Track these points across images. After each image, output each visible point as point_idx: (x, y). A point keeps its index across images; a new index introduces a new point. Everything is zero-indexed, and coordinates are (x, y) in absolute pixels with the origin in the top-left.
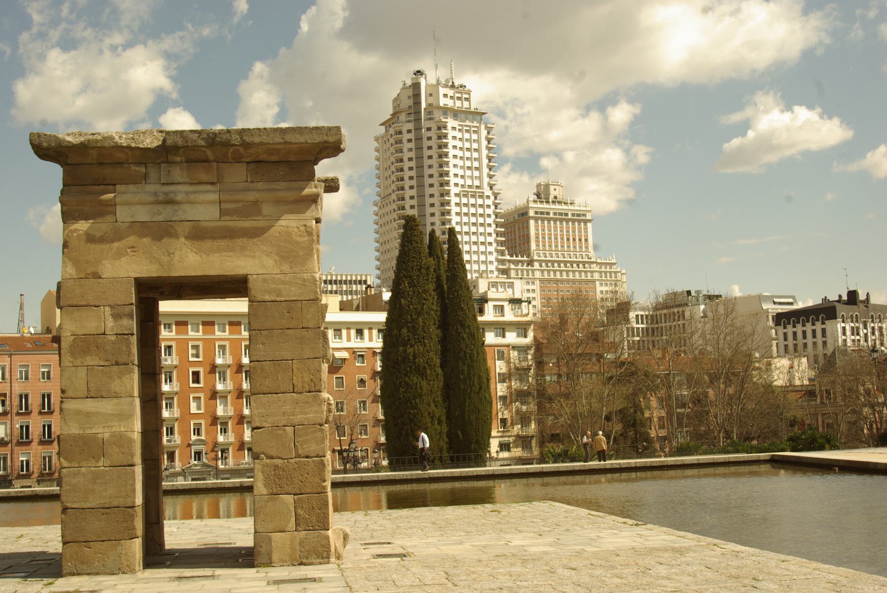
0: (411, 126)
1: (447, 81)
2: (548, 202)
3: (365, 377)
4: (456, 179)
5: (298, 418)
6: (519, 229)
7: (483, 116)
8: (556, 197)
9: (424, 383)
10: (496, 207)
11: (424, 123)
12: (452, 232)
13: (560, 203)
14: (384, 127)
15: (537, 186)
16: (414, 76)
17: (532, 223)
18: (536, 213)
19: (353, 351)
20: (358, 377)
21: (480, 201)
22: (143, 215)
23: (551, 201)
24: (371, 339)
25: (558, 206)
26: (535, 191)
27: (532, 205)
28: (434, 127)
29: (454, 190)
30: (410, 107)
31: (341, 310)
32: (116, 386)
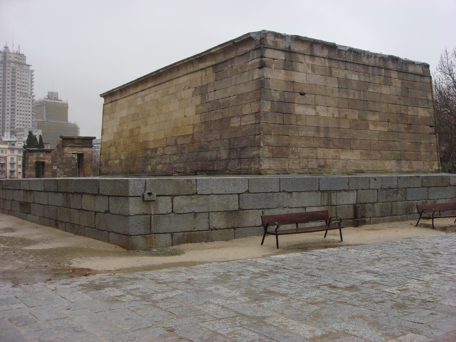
1: (17, 52)
2: (52, 99)
4: (18, 90)
6: (40, 109)
7: (30, 67)
8: (55, 98)
10: (33, 102)
11: (8, 68)
13: (56, 100)
15: (48, 93)
16: (4, 49)
21: (27, 99)
23: (53, 99)
25: (55, 101)
26: (47, 94)
30: (2, 61)
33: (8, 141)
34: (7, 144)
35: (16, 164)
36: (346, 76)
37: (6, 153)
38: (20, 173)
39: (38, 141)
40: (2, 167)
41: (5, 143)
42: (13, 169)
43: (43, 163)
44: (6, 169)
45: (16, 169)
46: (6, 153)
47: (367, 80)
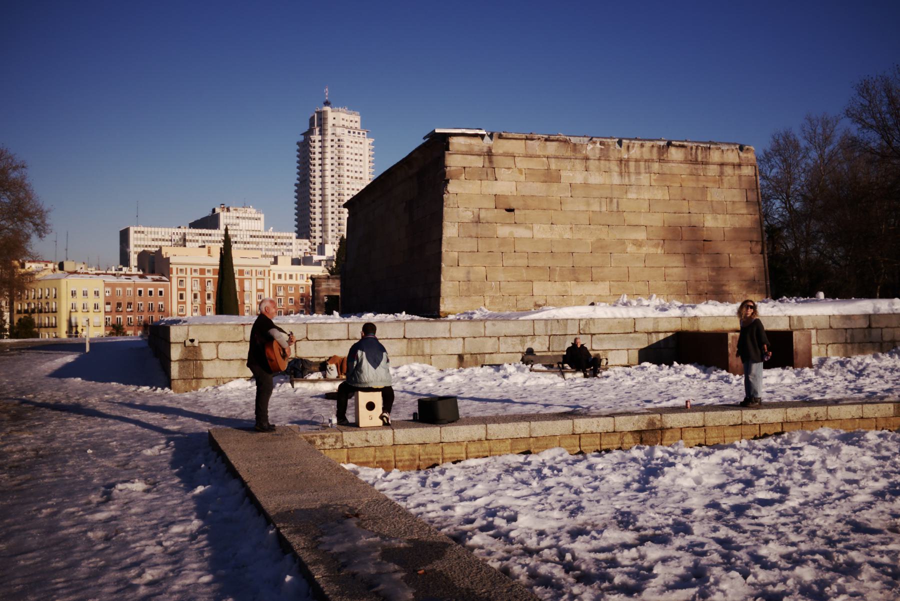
14: (303, 137)
28: (336, 139)
29: (346, 180)
36: (586, 178)
47: (626, 181)
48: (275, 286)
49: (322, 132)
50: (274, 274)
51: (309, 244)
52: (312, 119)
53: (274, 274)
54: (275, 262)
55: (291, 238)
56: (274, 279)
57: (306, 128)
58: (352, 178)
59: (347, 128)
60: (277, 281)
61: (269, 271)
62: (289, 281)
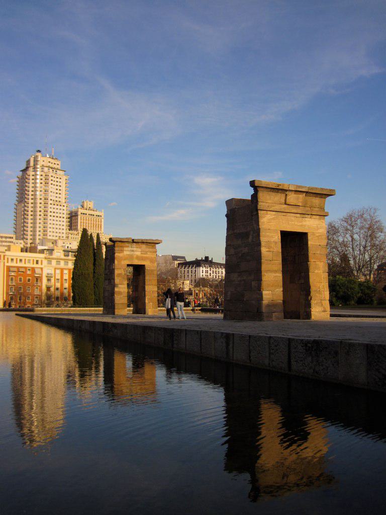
0: (33, 173)
3: (30, 278)
5: (153, 290)
9: (87, 283)
12: (98, 235)
17: (79, 217)
18: (81, 213)
19: (26, 268)
20: (28, 278)
22: (128, 253)
24: (33, 264)
26: (82, 204)
27: (79, 210)
28: (44, 175)
31: (22, 251)
32: (124, 283)
33: (45, 249)
34: (44, 253)
35: (54, 277)
37: (42, 264)
38: (57, 289)
39: (95, 242)
40: (37, 281)
41: (42, 251)
42: (49, 285)
43: (143, 267)
44: (42, 283)
45: (54, 284)
46: (42, 264)
48: (9, 267)
49: (35, 168)
50: (8, 258)
51: (23, 243)
52: (28, 162)
53: (8, 258)
54: (9, 250)
55: (12, 238)
56: (8, 262)
57: (24, 167)
58: (54, 201)
59: (52, 168)
60: (10, 264)
61: (4, 256)
62: (19, 264)
